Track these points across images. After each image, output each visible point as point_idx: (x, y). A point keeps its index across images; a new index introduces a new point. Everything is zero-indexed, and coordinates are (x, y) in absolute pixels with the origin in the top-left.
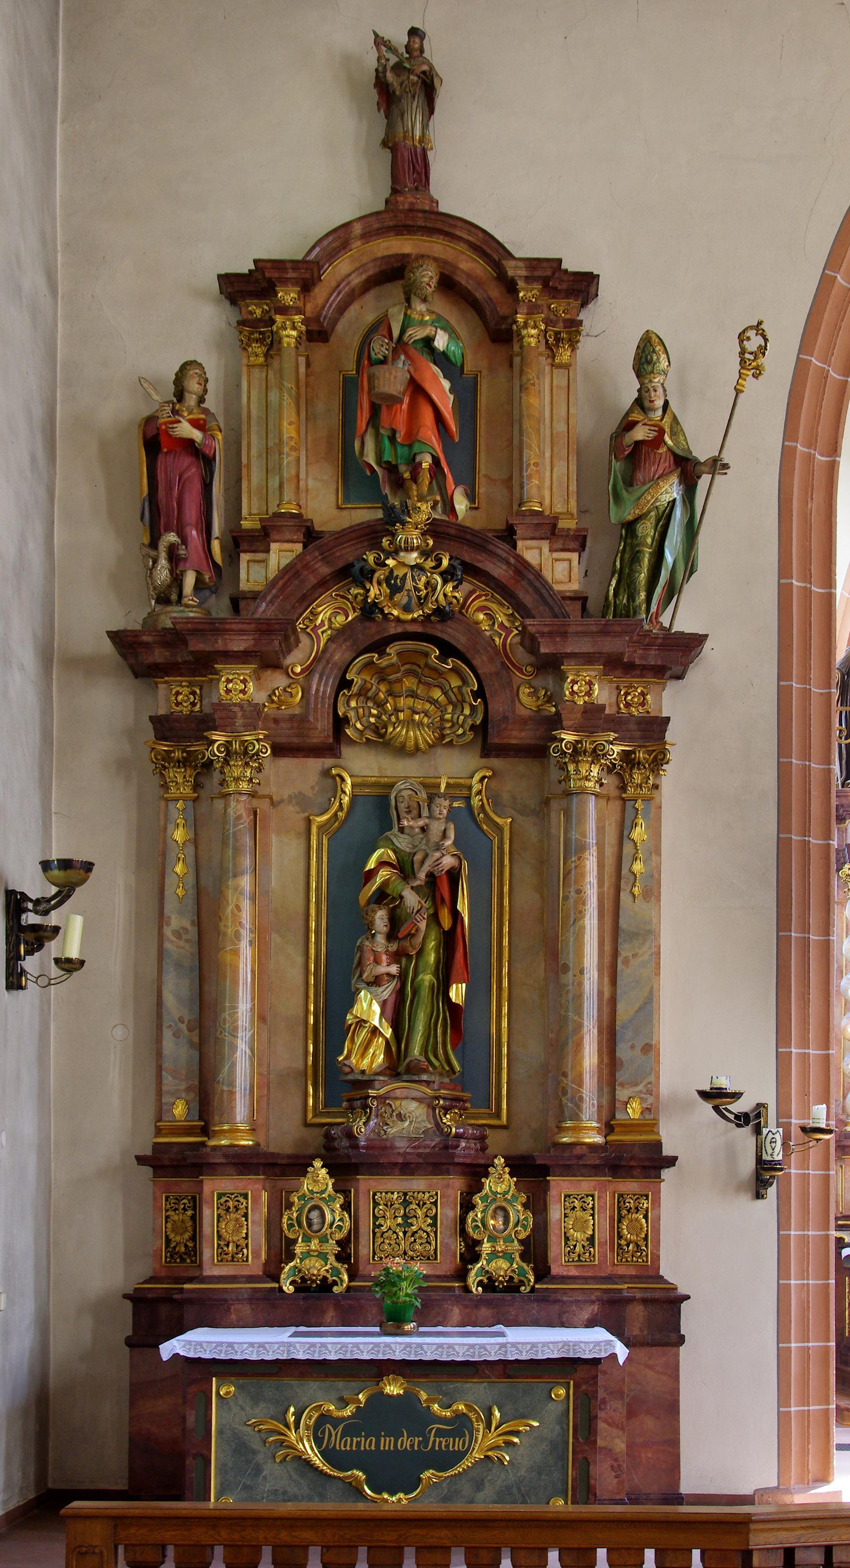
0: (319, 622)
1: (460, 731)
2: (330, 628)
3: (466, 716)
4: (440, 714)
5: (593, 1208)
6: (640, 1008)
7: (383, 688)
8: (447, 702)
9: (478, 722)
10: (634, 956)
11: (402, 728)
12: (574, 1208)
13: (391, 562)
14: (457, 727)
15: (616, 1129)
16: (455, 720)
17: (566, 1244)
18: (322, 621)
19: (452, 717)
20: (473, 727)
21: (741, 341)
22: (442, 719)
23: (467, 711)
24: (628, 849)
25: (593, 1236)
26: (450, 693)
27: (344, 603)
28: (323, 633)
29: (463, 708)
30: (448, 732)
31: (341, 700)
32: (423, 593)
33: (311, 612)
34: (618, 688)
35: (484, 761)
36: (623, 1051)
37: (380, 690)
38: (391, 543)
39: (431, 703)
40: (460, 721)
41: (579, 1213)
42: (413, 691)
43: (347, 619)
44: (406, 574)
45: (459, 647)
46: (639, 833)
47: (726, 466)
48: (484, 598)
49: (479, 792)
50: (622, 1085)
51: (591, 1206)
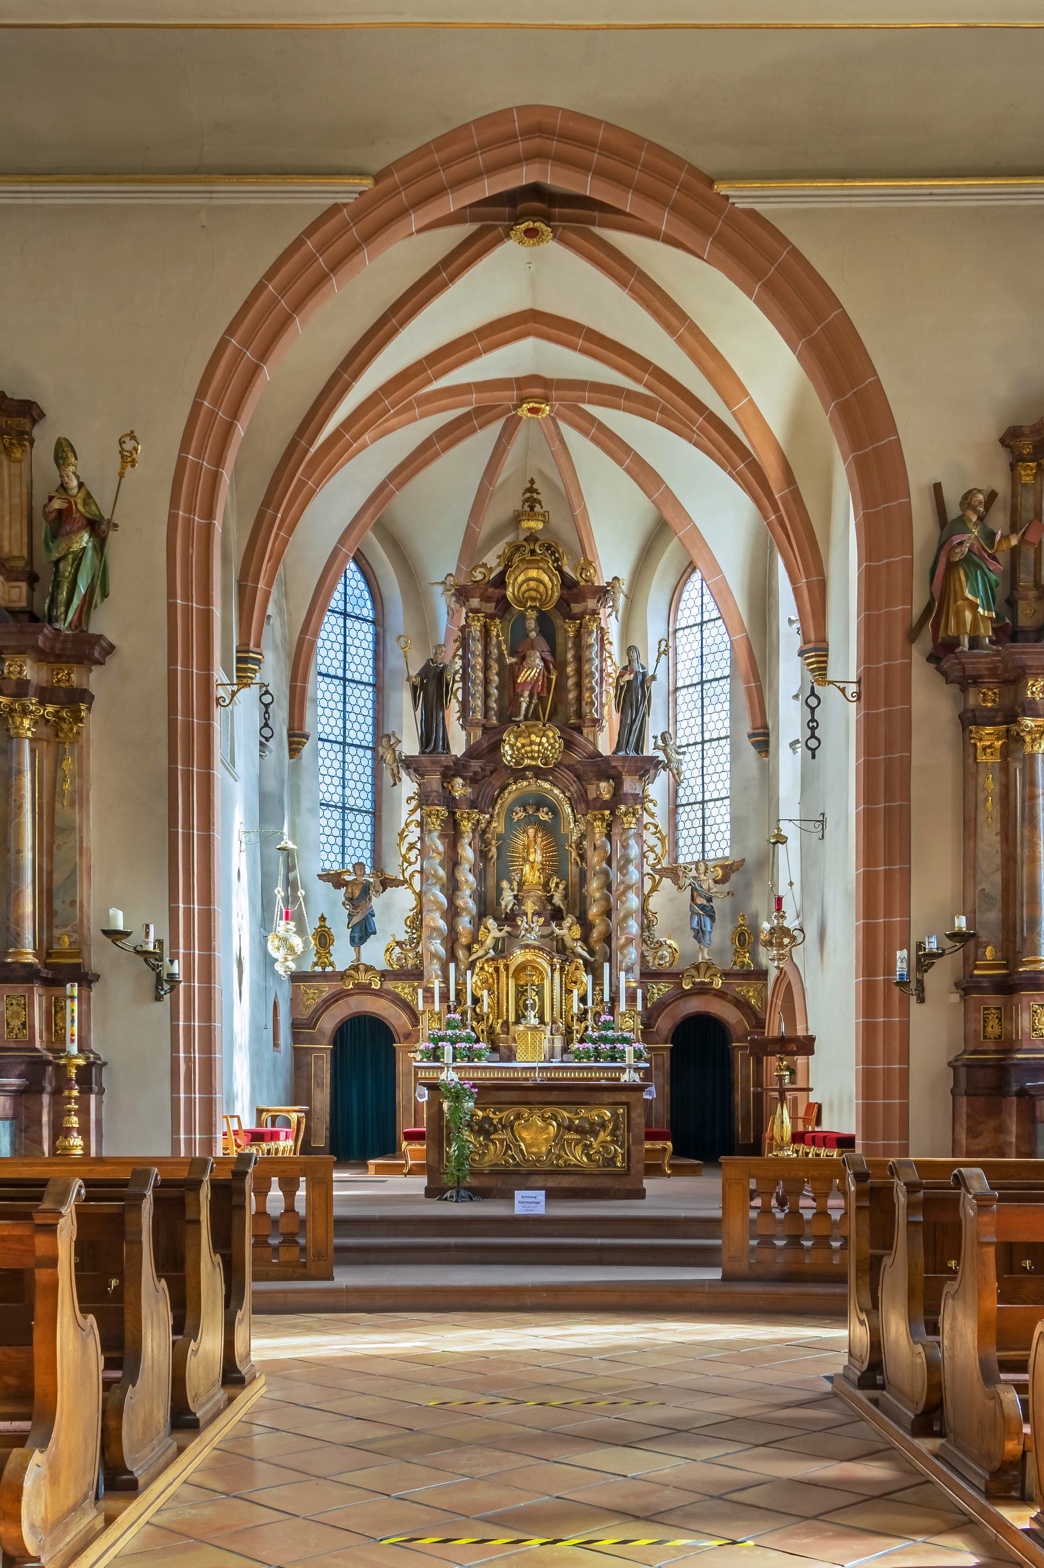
5: (25, 1004)
6: (67, 878)
10: (65, 843)
12: (12, 1004)
15: (53, 955)
17: (8, 1027)
21: (121, 445)
24: (60, 774)
25: (25, 1022)
34: (52, 670)
36: (57, 905)
41: (15, 1008)
46: (68, 764)
47: (116, 525)
50: (57, 927)
51: (23, 1002)
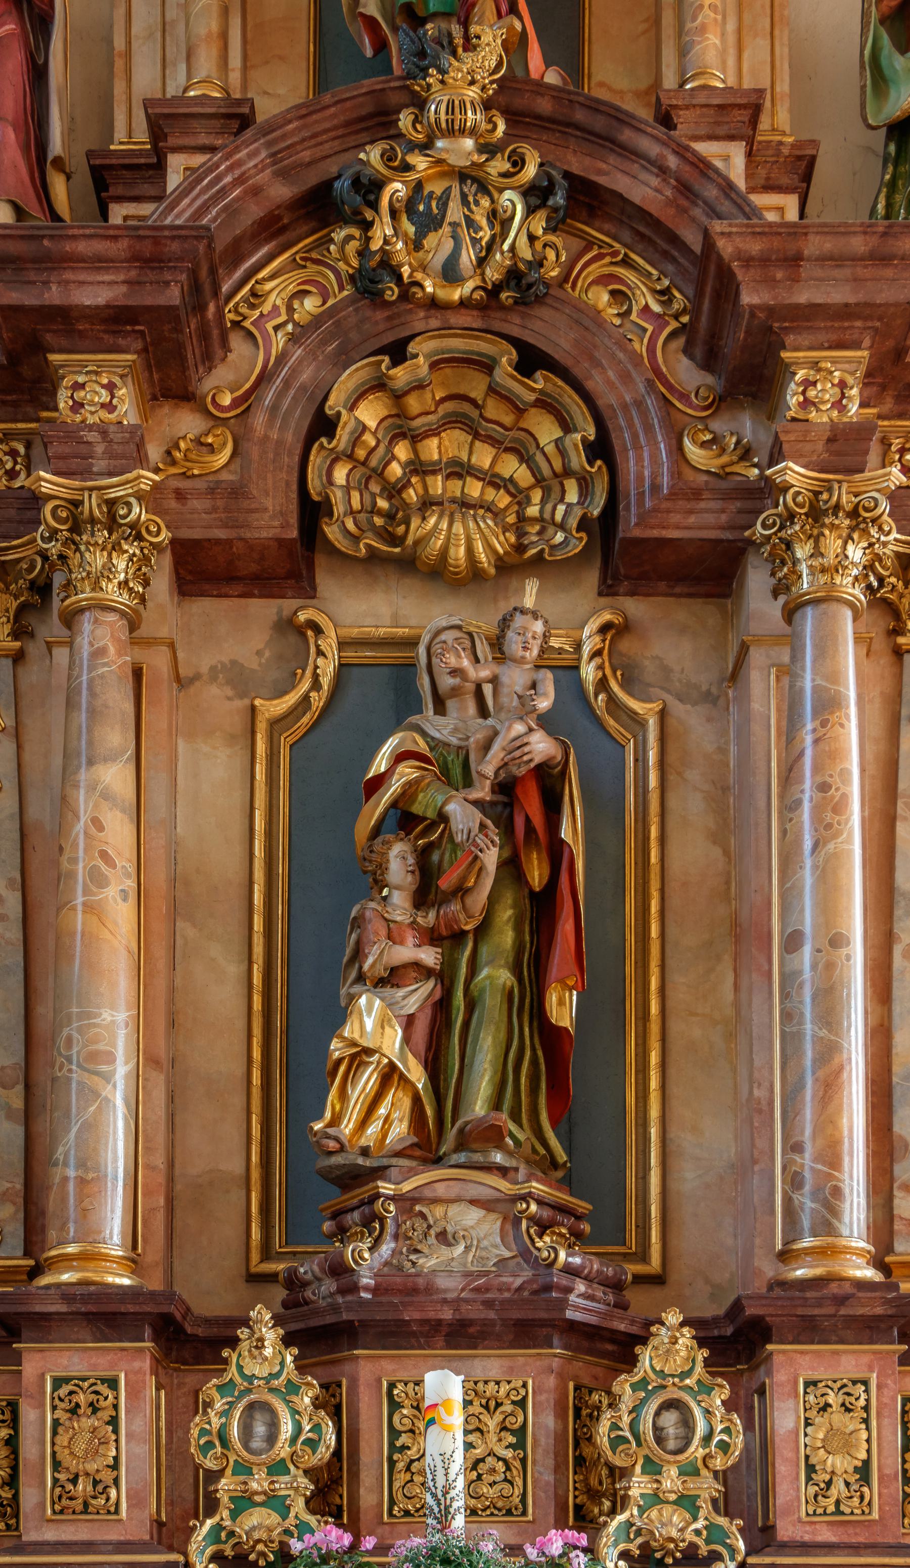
0: (267, 308)
1: (559, 537)
2: (290, 319)
3: (569, 505)
4: (516, 508)
7: (402, 451)
8: (532, 480)
9: (596, 513)
11: (440, 517)
13: (420, 162)
14: (551, 530)
16: (547, 516)
18: (275, 307)
19: (541, 511)
20: (584, 524)
22: (522, 518)
23: (572, 496)
26: (539, 458)
27: (320, 273)
28: (276, 328)
29: (563, 492)
30: (534, 538)
31: (316, 460)
32: (485, 234)
33: (253, 293)
35: (604, 601)
37: (394, 457)
38: (416, 121)
39: (497, 487)
40: (559, 517)
42: (460, 464)
43: (324, 303)
44: (447, 191)
45: (556, 356)
48: (608, 259)
49: (597, 653)
